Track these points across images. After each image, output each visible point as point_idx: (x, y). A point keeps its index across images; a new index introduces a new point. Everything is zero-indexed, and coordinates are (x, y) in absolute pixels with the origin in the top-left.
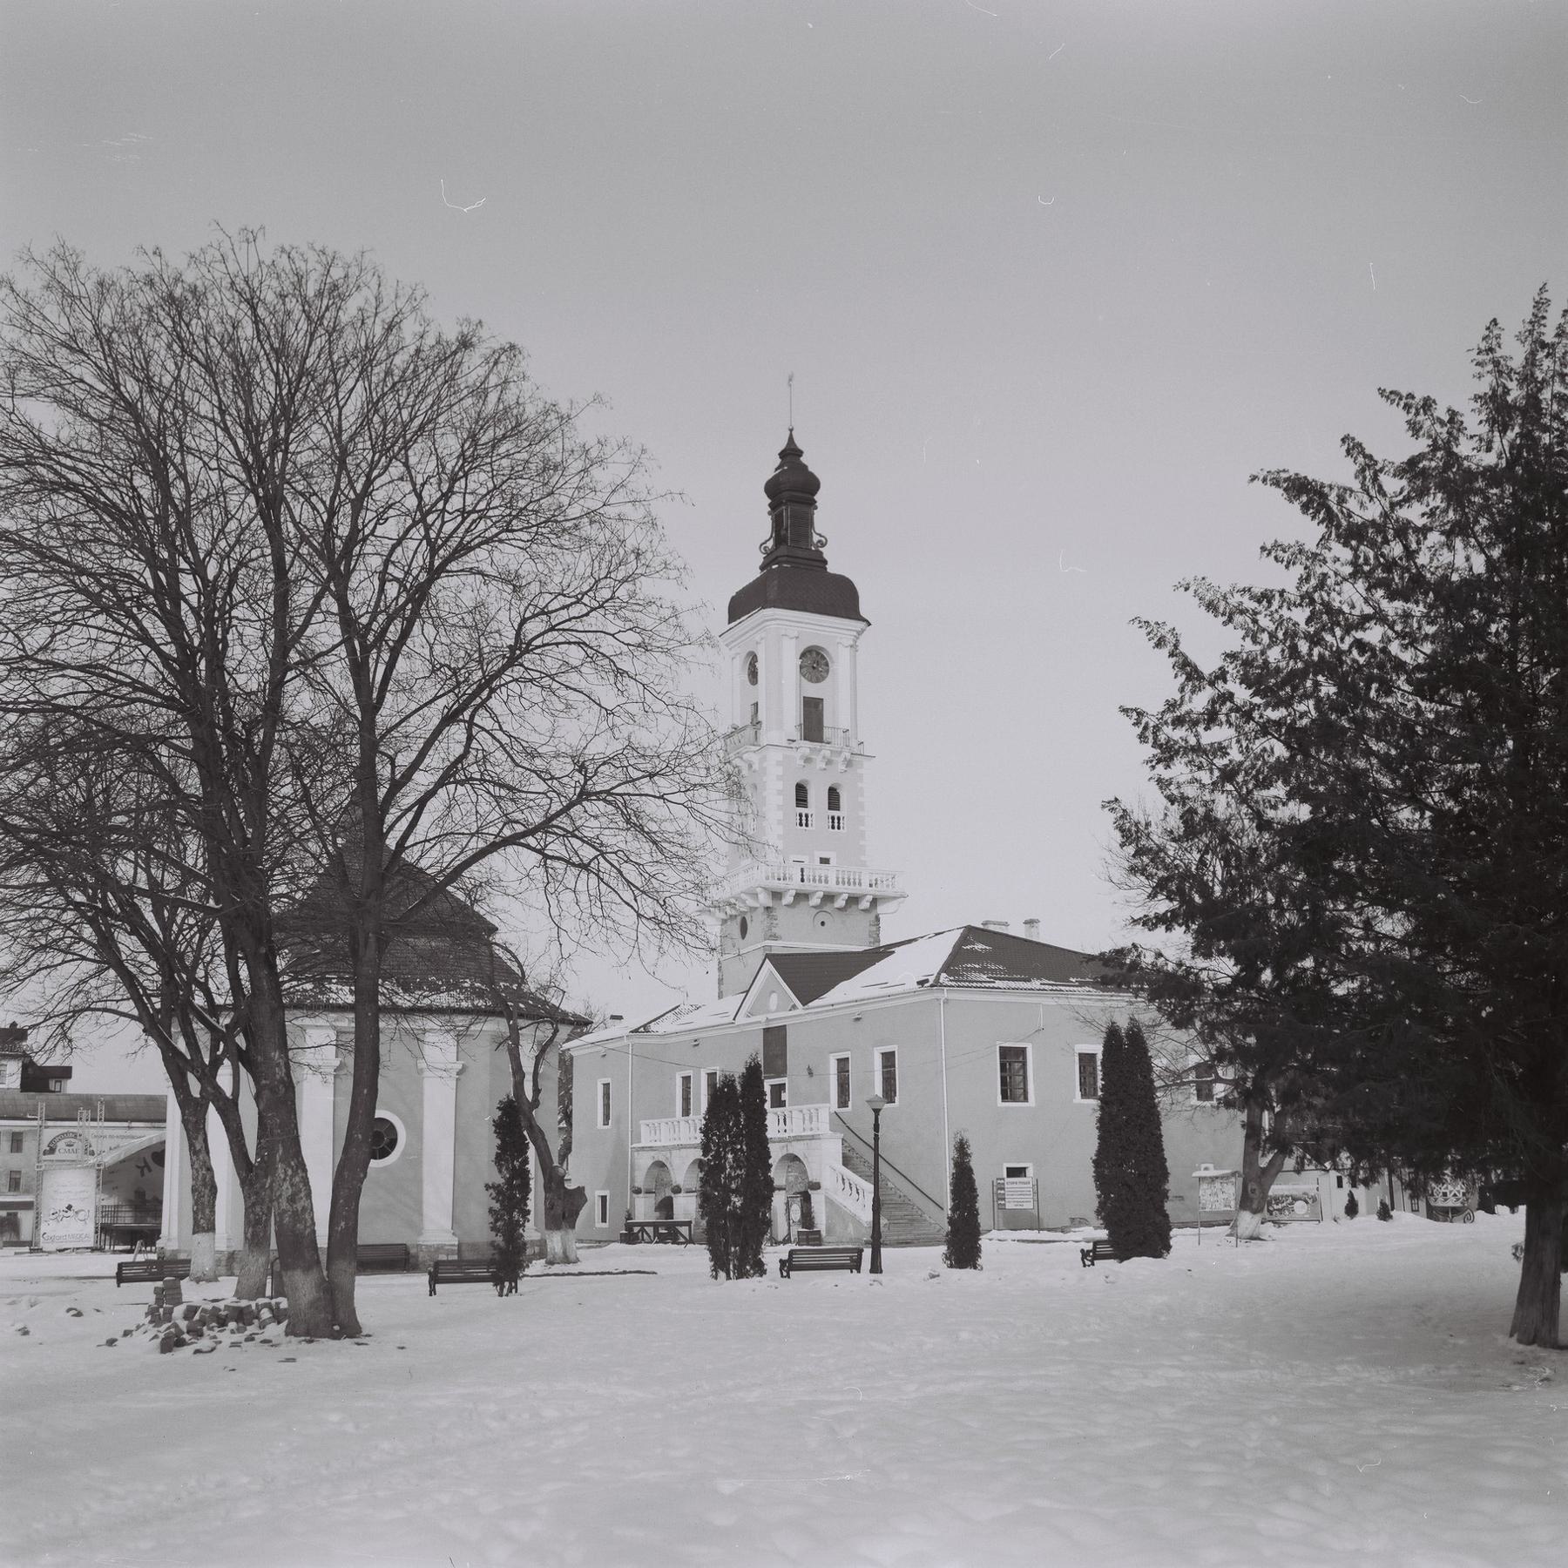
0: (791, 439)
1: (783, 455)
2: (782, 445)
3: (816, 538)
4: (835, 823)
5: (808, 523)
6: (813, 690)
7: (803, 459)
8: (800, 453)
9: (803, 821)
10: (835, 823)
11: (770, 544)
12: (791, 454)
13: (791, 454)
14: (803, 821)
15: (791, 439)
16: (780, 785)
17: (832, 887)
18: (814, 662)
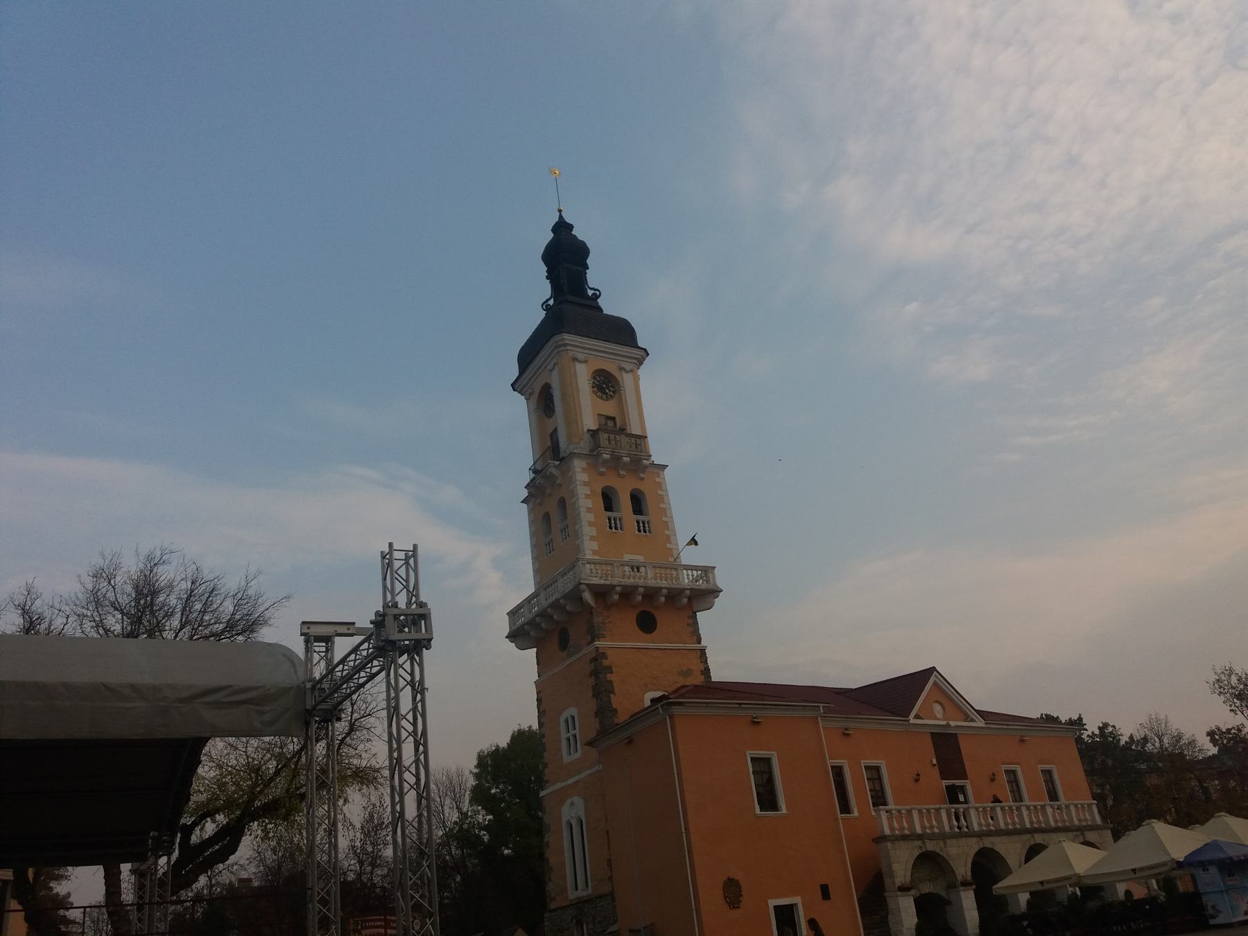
0: (561, 217)
1: (555, 229)
3: (590, 293)
4: (643, 527)
5: (584, 280)
6: (609, 408)
8: (571, 227)
10: (643, 527)
11: (551, 302)
12: (562, 228)
13: (562, 228)
14: (614, 524)
15: (561, 217)
16: (587, 491)
17: (651, 582)
18: (606, 384)
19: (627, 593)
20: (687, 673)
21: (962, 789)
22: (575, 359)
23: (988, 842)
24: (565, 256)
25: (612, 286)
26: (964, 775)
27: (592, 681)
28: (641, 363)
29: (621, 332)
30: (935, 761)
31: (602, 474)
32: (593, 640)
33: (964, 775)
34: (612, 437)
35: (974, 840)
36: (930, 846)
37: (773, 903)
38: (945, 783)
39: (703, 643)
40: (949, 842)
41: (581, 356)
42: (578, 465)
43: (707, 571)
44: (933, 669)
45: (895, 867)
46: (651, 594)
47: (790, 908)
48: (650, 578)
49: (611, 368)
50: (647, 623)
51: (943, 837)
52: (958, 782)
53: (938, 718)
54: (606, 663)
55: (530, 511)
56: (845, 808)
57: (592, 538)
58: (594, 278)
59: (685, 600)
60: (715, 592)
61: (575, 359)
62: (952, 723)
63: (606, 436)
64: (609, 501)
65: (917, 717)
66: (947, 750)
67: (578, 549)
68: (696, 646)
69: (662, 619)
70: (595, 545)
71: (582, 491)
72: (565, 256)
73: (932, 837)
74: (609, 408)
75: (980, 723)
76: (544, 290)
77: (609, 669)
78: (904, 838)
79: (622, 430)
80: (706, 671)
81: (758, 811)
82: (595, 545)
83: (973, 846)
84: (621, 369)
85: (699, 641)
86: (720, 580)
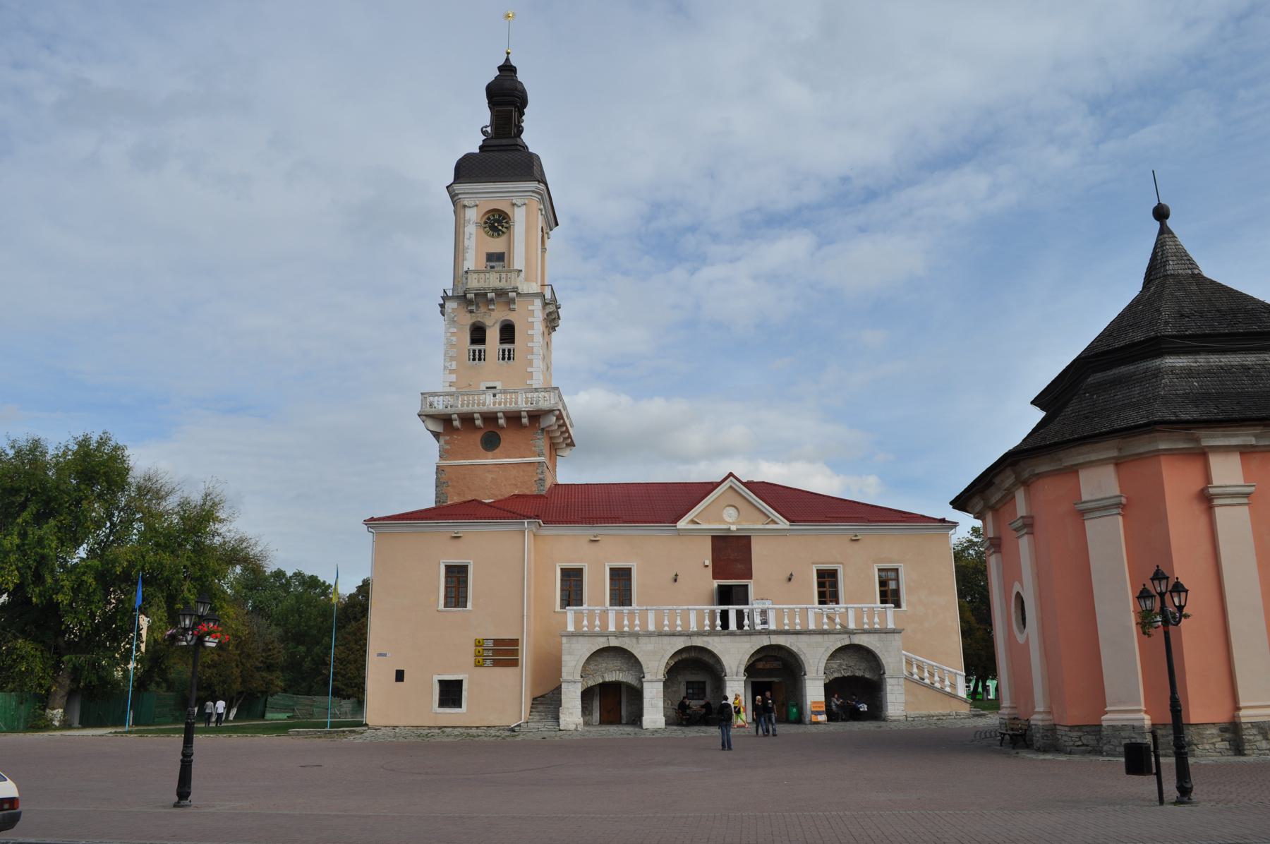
0: (507, 59)
4: (507, 356)
9: (479, 357)
12: (507, 69)
13: (507, 69)
15: (507, 59)
19: (467, 419)
23: (698, 642)
24: (506, 97)
26: (750, 577)
30: (707, 563)
31: (471, 312)
33: (748, 575)
34: (482, 276)
35: (682, 639)
36: (614, 642)
37: (436, 678)
38: (716, 583)
40: (643, 640)
44: (731, 474)
45: (564, 658)
46: (490, 418)
47: (459, 683)
48: (490, 403)
50: (491, 442)
51: (636, 636)
53: (730, 520)
59: (525, 421)
61: (465, 206)
62: (733, 528)
63: (475, 276)
64: (478, 334)
65: (693, 522)
66: (731, 555)
69: (507, 438)
70: (453, 377)
72: (506, 97)
73: (620, 634)
74: (497, 245)
75: (784, 524)
78: (583, 635)
81: (441, 606)
82: (453, 377)
83: (680, 643)
84: (514, 205)
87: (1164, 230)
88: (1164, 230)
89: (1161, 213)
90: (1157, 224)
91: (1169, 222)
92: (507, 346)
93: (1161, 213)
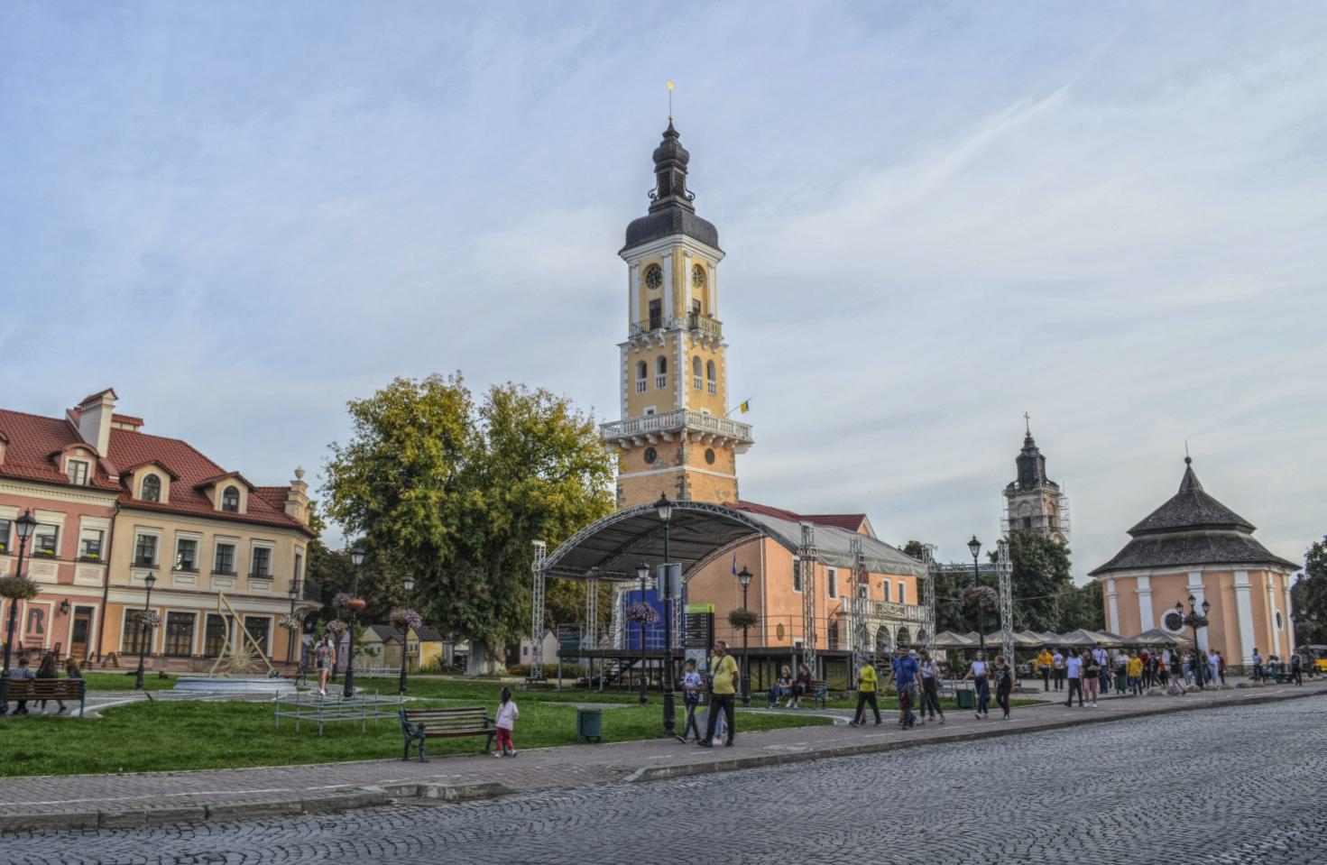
0: (671, 125)
2: (665, 128)
3: (687, 194)
4: (712, 389)
7: (680, 140)
8: (677, 135)
11: (656, 192)
12: (670, 134)
13: (670, 134)
14: (697, 385)
15: (671, 125)
18: (700, 274)
20: (727, 494)
21: (865, 589)
22: (685, 254)
24: (670, 160)
25: (706, 195)
27: (678, 490)
28: (719, 260)
29: (708, 235)
32: (681, 463)
39: (737, 475)
41: (689, 253)
42: (684, 337)
43: (745, 428)
49: (704, 265)
50: (710, 457)
52: (864, 585)
54: (688, 481)
55: (623, 354)
56: (832, 594)
57: (686, 394)
58: (690, 184)
60: (750, 443)
61: (685, 254)
67: (675, 399)
68: (732, 477)
71: (684, 358)
76: (652, 183)
77: (690, 485)
79: (710, 316)
80: (737, 495)
84: (709, 265)
85: (734, 474)
86: (753, 435)
87: (1189, 469)
88: (1189, 469)
89: (1188, 460)
90: (1186, 466)
91: (1191, 465)
92: (711, 382)
93: (1188, 460)
